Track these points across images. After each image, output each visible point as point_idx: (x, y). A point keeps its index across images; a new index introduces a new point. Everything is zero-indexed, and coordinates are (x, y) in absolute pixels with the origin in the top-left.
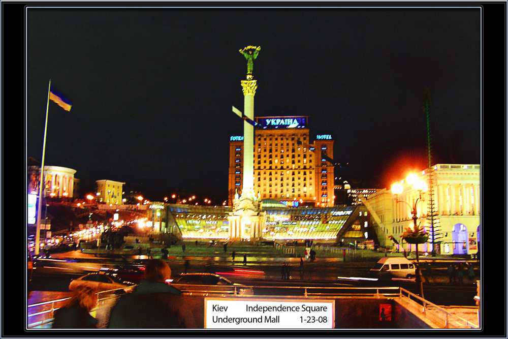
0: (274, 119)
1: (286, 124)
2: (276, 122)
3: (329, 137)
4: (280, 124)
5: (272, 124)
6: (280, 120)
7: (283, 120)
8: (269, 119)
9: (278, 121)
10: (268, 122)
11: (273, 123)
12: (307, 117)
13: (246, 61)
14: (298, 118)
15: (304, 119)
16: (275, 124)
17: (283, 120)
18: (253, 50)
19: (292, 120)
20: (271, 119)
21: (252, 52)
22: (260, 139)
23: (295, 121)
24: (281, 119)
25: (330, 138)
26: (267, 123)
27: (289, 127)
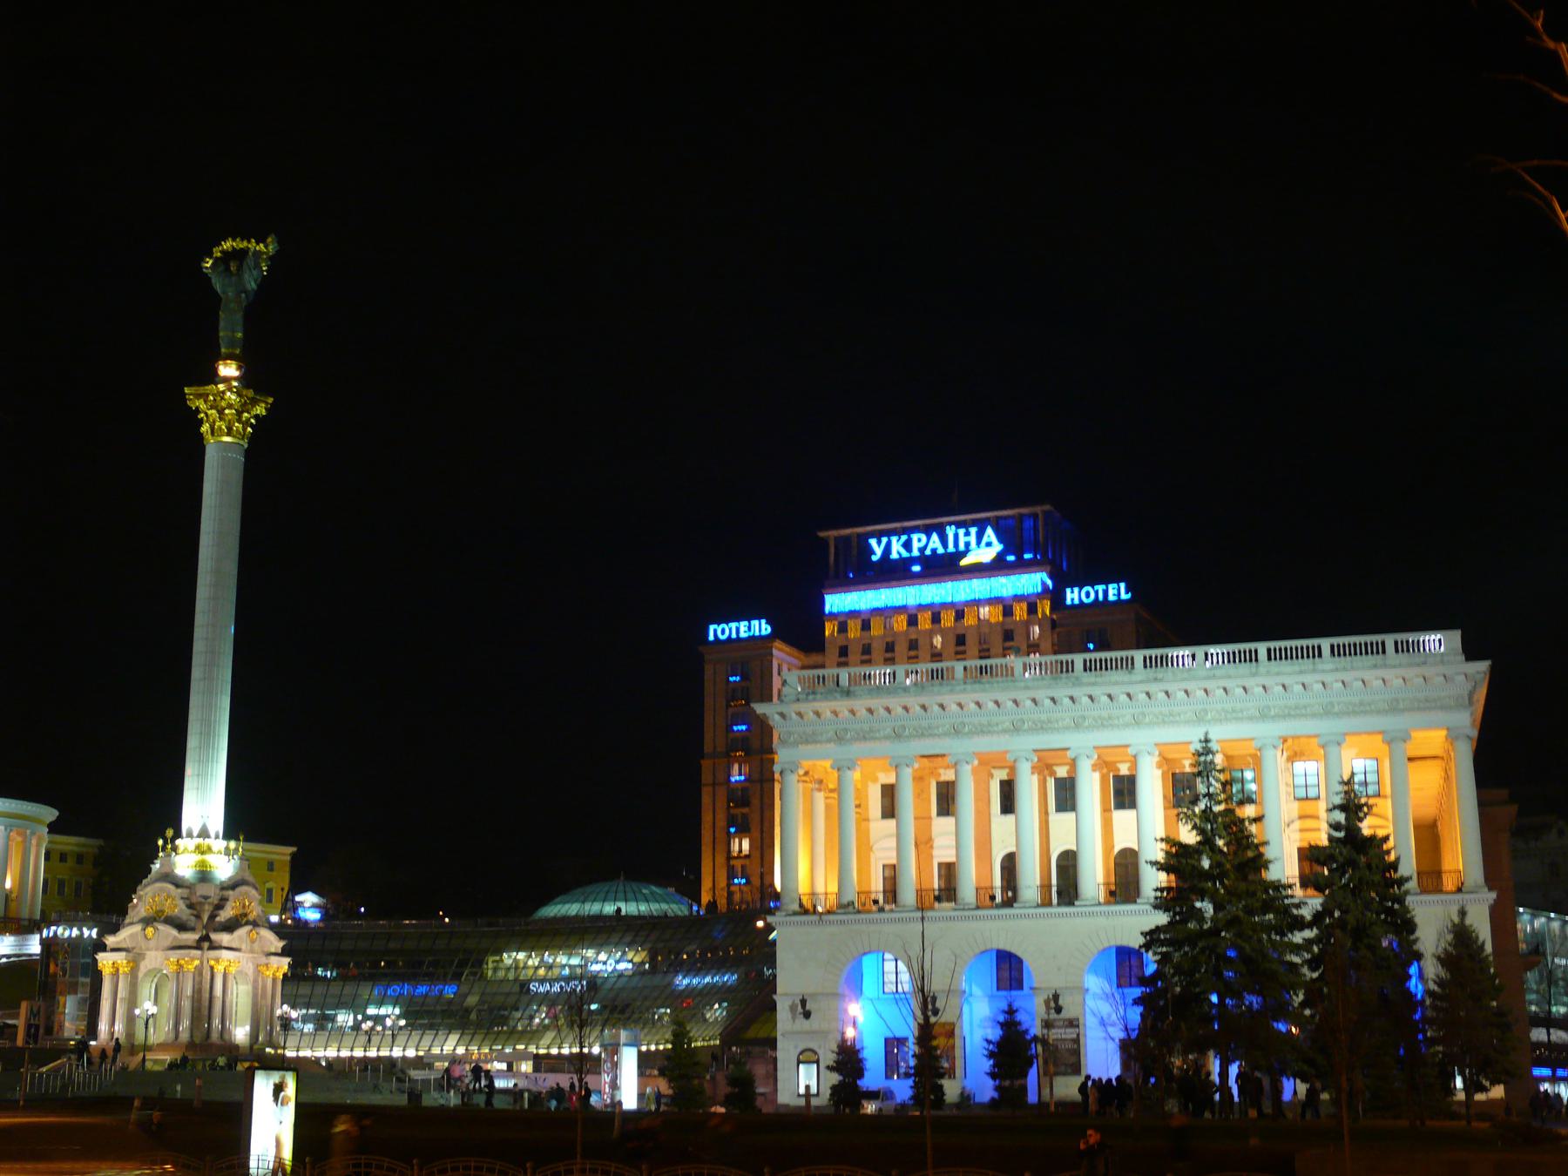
0: (898, 533)
1: (951, 549)
2: (907, 545)
3: (1117, 592)
4: (928, 552)
5: (894, 556)
6: (924, 537)
7: (935, 537)
8: (879, 535)
9: (918, 540)
10: (878, 551)
11: (897, 551)
12: (1038, 509)
13: (213, 302)
14: (997, 518)
15: (1029, 524)
16: (905, 554)
17: (935, 537)
18: (239, 255)
19: (973, 530)
20: (889, 533)
21: (240, 261)
22: (843, 628)
23: (990, 533)
24: (928, 531)
25: (1124, 596)
26: (873, 553)
27: (964, 562)
